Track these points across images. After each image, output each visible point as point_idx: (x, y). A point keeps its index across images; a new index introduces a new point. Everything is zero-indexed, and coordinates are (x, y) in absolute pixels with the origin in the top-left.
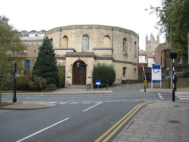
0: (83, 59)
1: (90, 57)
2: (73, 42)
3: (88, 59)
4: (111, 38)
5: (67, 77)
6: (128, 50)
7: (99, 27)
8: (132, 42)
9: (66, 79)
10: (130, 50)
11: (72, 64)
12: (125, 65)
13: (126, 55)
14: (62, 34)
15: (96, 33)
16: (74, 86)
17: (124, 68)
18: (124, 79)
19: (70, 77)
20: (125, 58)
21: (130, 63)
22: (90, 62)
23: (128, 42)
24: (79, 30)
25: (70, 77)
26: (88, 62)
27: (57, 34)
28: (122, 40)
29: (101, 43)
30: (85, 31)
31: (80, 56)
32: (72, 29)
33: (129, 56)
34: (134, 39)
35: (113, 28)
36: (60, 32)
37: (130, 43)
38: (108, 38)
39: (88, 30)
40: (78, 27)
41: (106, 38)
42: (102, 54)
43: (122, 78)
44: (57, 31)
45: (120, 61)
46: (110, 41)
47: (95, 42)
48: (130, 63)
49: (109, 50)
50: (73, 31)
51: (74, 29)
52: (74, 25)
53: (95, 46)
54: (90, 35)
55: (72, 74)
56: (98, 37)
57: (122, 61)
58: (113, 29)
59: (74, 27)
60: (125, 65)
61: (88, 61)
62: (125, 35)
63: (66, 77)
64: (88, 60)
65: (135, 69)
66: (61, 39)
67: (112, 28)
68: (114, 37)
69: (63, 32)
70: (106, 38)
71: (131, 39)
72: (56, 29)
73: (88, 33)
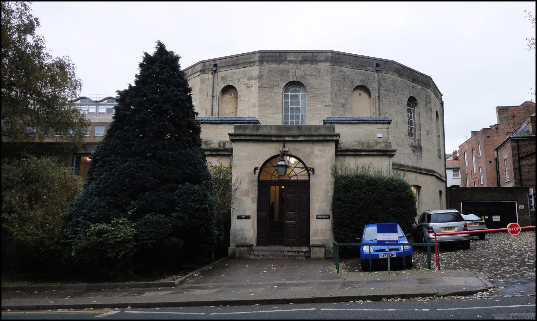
1: (324, 144)
2: (254, 106)
4: (374, 94)
5: (239, 218)
6: (422, 133)
7: (337, 58)
8: (431, 109)
9: (236, 224)
10: (428, 134)
11: (255, 169)
12: (416, 179)
13: (417, 148)
14: (219, 80)
15: (330, 77)
16: (260, 248)
19: (248, 218)
20: (414, 157)
22: (324, 160)
23: (420, 109)
24: (274, 67)
25: (248, 218)
27: (202, 81)
28: (406, 103)
29: (343, 106)
30: (292, 69)
31: (287, 138)
32: (250, 63)
33: (425, 151)
34: (434, 105)
35: (378, 62)
36: (211, 76)
37: (427, 114)
38: (364, 95)
39: (303, 67)
40: (269, 56)
41: (360, 94)
42: (356, 139)
44: (201, 71)
45: (403, 166)
47: (324, 104)
49: (379, 126)
50: (255, 70)
53: (327, 114)
54: (309, 81)
55: (255, 206)
56: (336, 88)
57: (408, 167)
59: (256, 58)
60: (416, 179)
62: (413, 87)
63: (234, 217)
64: (316, 152)
65: (441, 192)
66: (213, 97)
67: (377, 65)
68: (383, 92)
69: (221, 74)
70: (360, 94)
71: (428, 101)
72: (199, 67)
73: (304, 77)
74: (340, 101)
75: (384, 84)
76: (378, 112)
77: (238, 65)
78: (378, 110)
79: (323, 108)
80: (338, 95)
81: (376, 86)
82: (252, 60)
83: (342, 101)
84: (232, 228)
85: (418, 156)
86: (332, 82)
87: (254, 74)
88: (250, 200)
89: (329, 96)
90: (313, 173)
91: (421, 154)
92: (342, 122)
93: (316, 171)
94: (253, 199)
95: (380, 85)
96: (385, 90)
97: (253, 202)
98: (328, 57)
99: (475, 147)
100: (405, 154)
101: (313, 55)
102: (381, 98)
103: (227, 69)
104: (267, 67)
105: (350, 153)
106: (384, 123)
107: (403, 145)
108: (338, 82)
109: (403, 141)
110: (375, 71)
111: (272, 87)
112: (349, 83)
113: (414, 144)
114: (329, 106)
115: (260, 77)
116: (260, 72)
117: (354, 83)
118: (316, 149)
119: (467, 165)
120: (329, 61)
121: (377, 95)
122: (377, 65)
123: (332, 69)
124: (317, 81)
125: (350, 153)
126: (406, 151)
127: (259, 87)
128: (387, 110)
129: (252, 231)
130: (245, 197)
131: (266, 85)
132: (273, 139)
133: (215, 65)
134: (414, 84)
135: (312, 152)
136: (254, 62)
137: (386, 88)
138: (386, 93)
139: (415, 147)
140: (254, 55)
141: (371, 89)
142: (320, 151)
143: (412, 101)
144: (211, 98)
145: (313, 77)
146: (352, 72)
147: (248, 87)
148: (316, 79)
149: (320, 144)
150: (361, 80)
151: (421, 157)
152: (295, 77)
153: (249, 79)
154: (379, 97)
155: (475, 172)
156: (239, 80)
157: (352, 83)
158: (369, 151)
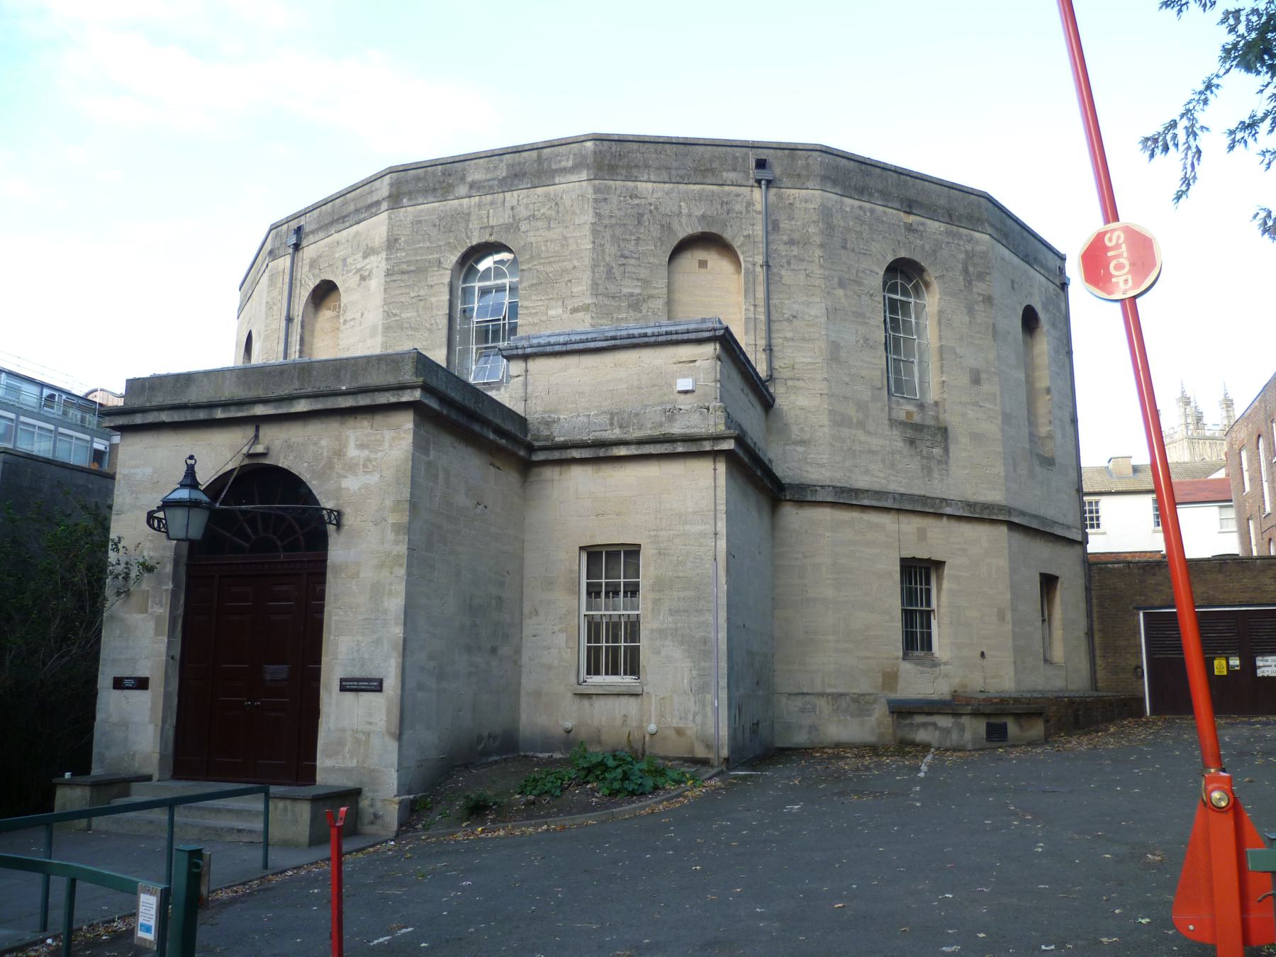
0: (292, 448)
1: (379, 419)
3: (355, 438)
5: (119, 684)
7: (614, 156)
14: (306, 269)
15: (589, 217)
17: (918, 574)
18: (918, 683)
19: (142, 684)
20: (914, 465)
21: (979, 514)
22: (373, 479)
24: (429, 208)
25: (142, 684)
26: (351, 483)
28: (877, 281)
30: (480, 206)
31: (260, 410)
33: (964, 440)
35: (763, 154)
38: (718, 263)
39: (511, 198)
42: (606, 405)
43: (890, 678)
45: (857, 492)
46: (749, 290)
47: (571, 304)
48: (979, 514)
50: (377, 227)
51: (385, 205)
52: (380, 176)
54: (533, 235)
56: (611, 249)
57: (878, 494)
58: (766, 164)
61: (351, 468)
62: (910, 228)
63: (104, 682)
64: (352, 452)
66: (289, 320)
67: (761, 164)
69: (308, 252)
70: (703, 264)
73: (513, 227)
74: (625, 291)
75: (784, 225)
76: (762, 317)
77: (343, 218)
78: (761, 309)
79: (566, 316)
80: (617, 272)
81: (759, 230)
82: (375, 198)
83: (630, 288)
84: (99, 716)
85: (929, 457)
86: (595, 232)
87: (377, 242)
88: (152, 624)
89: (586, 277)
90: (339, 525)
91: (946, 450)
92: (557, 348)
93: (348, 520)
94: (158, 619)
95: (772, 226)
96: (792, 242)
97: (158, 632)
98: (584, 157)
99: (1263, 429)
100: (871, 452)
101: (539, 156)
102: (775, 270)
103: (321, 235)
104: (409, 212)
105: (576, 454)
106: (699, 342)
107: (861, 425)
108: (618, 231)
109: (862, 406)
110: (752, 182)
111: (421, 271)
112: (655, 231)
113: (917, 418)
114: (585, 308)
115: (392, 243)
116: (390, 229)
117: (676, 226)
118: (352, 444)
119: (1247, 488)
120: (588, 167)
121: (760, 259)
122: (761, 164)
123: (597, 190)
124: (551, 235)
125: (576, 454)
126: (876, 443)
127: (388, 274)
128: (795, 307)
129: (151, 728)
130: (139, 616)
131: (404, 267)
132: (219, 414)
133: (299, 230)
134: (911, 219)
135: (339, 453)
136: (378, 203)
137: (796, 236)
138: (795, 250)
139: (918, 428)
140: (378, 182)
141: (736, 244)
142: (361, 446)
143: (905, 274)
144: (283, 323)
145: (540, 224)
146: (668, 193)
147: (363, 278)
148: (549, 228)
149: (366, 423)
150: (703, 217)
151: (944, 461)
152: (488, 231)
153: (365, 256)
154: (767, 265)
155: (1268, 509)
156: (344, 260)
157: (667, 228)
158: (640, 442)
